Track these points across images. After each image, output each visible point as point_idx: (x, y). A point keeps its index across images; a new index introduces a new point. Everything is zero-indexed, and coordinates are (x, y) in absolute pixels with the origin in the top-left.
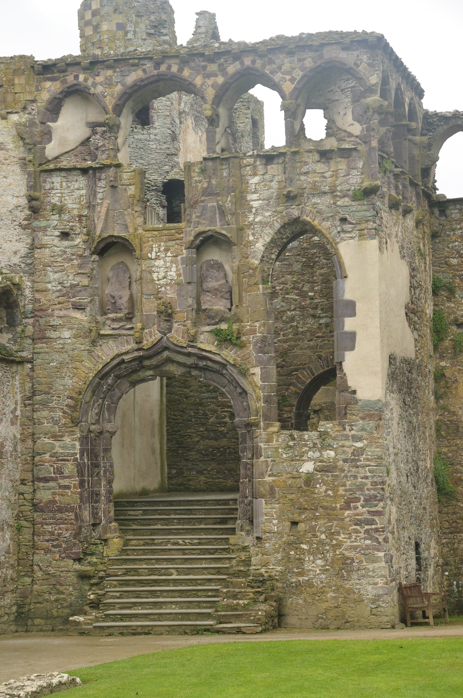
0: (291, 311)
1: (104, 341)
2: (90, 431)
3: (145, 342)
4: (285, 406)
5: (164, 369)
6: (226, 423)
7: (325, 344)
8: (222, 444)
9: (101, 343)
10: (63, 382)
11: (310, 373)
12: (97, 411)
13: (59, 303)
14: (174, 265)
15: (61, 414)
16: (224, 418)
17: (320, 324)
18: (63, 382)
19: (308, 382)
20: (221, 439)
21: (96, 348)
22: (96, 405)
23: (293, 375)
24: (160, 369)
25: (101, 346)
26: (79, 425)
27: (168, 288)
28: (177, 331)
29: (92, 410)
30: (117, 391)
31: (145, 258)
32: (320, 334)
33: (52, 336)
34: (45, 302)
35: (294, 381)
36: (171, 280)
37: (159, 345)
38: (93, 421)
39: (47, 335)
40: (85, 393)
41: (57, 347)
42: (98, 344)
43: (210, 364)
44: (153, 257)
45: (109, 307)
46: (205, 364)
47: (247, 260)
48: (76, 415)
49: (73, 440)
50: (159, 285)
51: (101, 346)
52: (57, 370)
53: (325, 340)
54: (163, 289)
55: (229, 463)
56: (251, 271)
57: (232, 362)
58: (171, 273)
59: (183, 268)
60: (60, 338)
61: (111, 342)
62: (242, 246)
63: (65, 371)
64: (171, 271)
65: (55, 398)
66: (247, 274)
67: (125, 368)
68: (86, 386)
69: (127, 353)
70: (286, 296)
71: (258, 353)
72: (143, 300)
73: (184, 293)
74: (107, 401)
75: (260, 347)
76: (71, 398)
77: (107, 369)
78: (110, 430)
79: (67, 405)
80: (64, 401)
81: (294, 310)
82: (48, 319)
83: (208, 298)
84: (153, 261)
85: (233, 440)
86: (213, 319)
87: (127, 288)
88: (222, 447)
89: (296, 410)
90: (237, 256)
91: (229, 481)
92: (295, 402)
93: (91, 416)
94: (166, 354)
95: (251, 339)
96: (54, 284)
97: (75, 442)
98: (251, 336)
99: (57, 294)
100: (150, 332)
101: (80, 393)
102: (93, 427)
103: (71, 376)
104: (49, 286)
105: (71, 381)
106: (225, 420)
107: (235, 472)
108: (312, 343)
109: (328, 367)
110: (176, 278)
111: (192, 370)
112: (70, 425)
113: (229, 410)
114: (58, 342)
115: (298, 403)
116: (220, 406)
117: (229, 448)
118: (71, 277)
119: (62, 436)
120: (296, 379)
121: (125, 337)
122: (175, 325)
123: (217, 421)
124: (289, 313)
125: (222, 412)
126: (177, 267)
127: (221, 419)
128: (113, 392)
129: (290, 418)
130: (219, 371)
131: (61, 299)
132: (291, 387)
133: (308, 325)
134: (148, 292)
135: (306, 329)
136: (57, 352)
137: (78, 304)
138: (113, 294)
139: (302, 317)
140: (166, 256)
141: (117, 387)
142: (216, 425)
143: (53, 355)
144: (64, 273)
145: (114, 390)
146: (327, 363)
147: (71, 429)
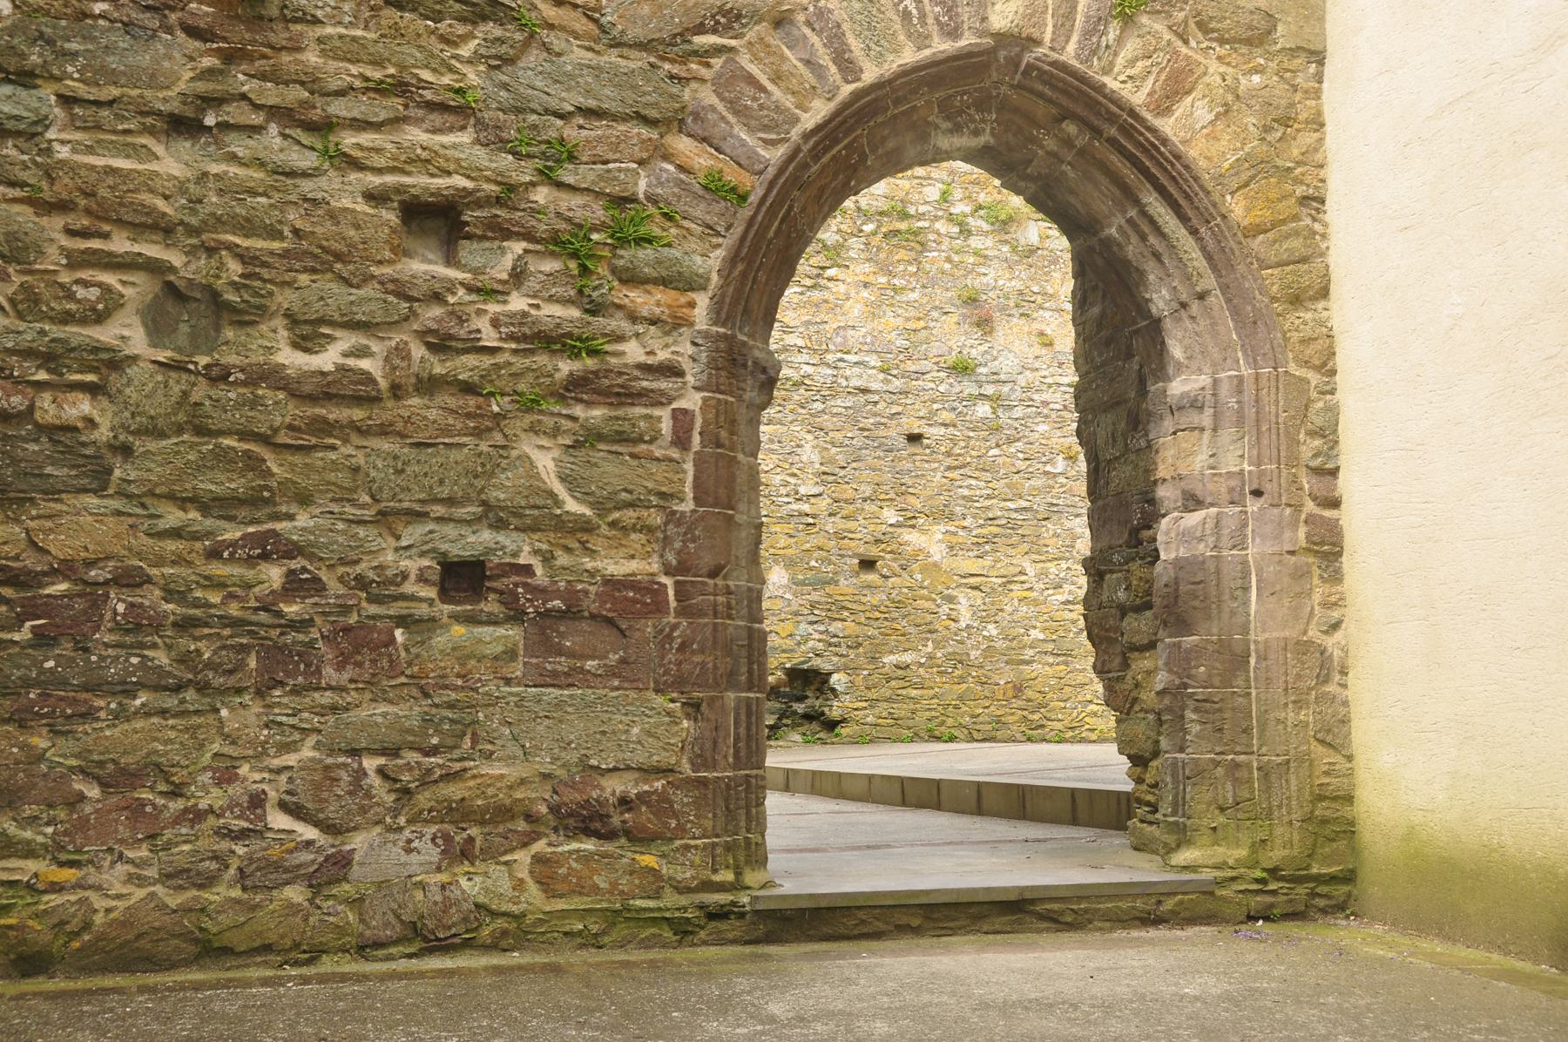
4: (630, 278)
6: (114, 362)
8: (61, 545)
11: (825, 58)
16: (100, 318)
19: (809, 120)
20: (53, 493)
23: (703, 55)
35: (708, 97)
55: (120, 715)
85: (173, 517)
88: (65, 569)
89: (720, 313)
91: (114, 877)
92: (710, 261)
106: (104, 334)
107: (176, 792)
109: (953, 33)
113: (152, 251)
115: (733, 260)
116: (62, 207)
117: (129, 580)
120: (721, 86)
123: (29, 333)
125: (77, 261)
127: (66, 318)
129: (671, 370)
132: (683, 145)
142: (18, 367)
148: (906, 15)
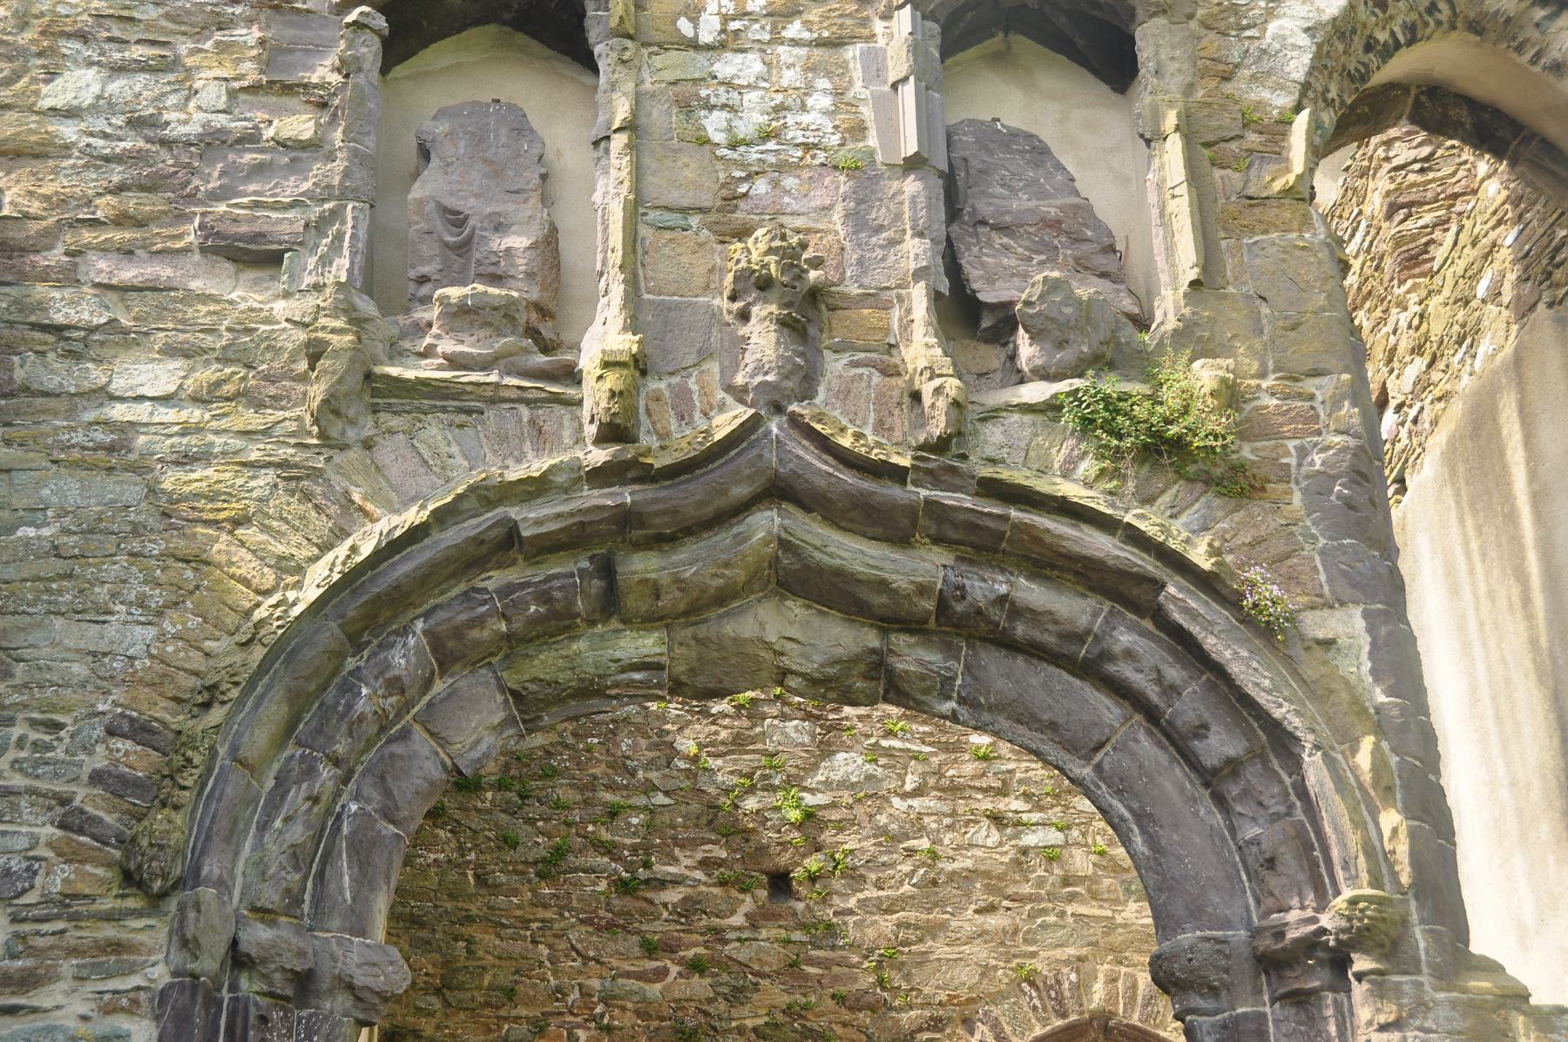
0: (905, 796)
1: (395, 422)
2: (238, 959)
3: (647, 440)
5: (729, 628)
7: (1044, 926)
9: (368, 432)
10: (90, 636)
12: (297, 833)
13: (122, 220)
14: (823, 83)
15: (49, 831)
17: (1025, 851)
18: (90, 636)
21: (338, 458)
22: (297, 796)
24: (702, 631)
25: (368, 445)
26: (172, 905)
27: (790, 182)
28: (844, 394)
29: (263, 827)
30: (421, 741)
31: (660, 37)
32: (1026, 889)
33: (51, 382)
34: (35, 207)
36: (807, 147)
37: (742, 461)
38: (270, 896)
39: (19, 374)
40: (240, 702)
41: (78, 438)
42: (352, 434)
43: (1032, 593)
44: (706, 37)
45: (426, 269)
46: (1003, 589)
47: (1228, 88)
48: (171, 826)
49: (109, 1010)
50: (742, 165)
51: (368, 445)
52: (61, 566)
53: (1044, 912)
54: (761, 186)
56: (1253, 138)
57: (1206, 565)
58: (805, 119)
59: (877, 99)
60: (104, 395)
61: (434, 432)
62: (1193, 25)
63: (112, 570)
64: (804, 108)
65: (16, 731)
66: (1233, 146)
67: (507, 590)
68: (258, 653)
69: (536, 488)
70: (885, 743)
71: (1335, 532)
72: (644, 231)
73: (879, 215)
74: (357, 797)
75: (1350, 505)
76: (141, 731)
77: (403, 568)
78: (360, 981)
79: (97, 778)
80: (88, 749)
81: (918, 792)
82: (40, 290)
83: (1007, 261)
84: (701, 58)
86: (1061, 344)
87: (534, 200)
90: (1173, 67)
93: (260, 866)
94: (765, 523)
95: (1293, 461)
96: (100, 124)
97: (124, 1023)
98: (1291, 445)
99: (117, 175)
100: (683, 394)
101: (210, 696)
102: (258, 935)
103: (157, 598)
104: (68, 131)
105: (151, 632)
108: (993, 921)
109: (1064, 1015)
110: (835, 139)
111: (901, 641)
112: (107, 904)
114: (89, 416)
118: (213, 95)
119: (28, 981)
121: (525, 412)
122: (836, 366)
124: (896, 801)
126: (838, 93)
128: (397, 749)
130: (1080, 638)
131: (132, 202)
133: (979, 853)
134: (674, 197)
135: (969, 863)
136: (76, 464)
137: (243, 229)
138: (452, 202)
139: (947, 821)
140: (777, 40)
141: (424, 720)
143: (39, 484)
144: (171, 77)
145: (405, 735)
146: (1060, 1000)
147: (108, 931)
148: (1035, 1008)
